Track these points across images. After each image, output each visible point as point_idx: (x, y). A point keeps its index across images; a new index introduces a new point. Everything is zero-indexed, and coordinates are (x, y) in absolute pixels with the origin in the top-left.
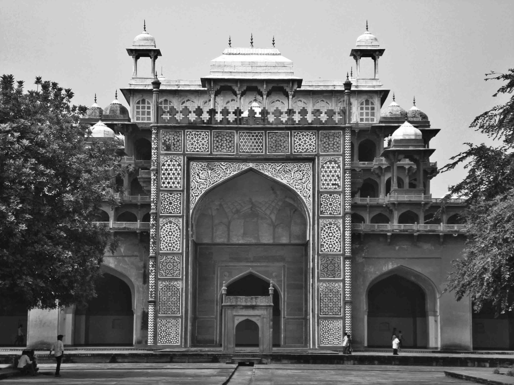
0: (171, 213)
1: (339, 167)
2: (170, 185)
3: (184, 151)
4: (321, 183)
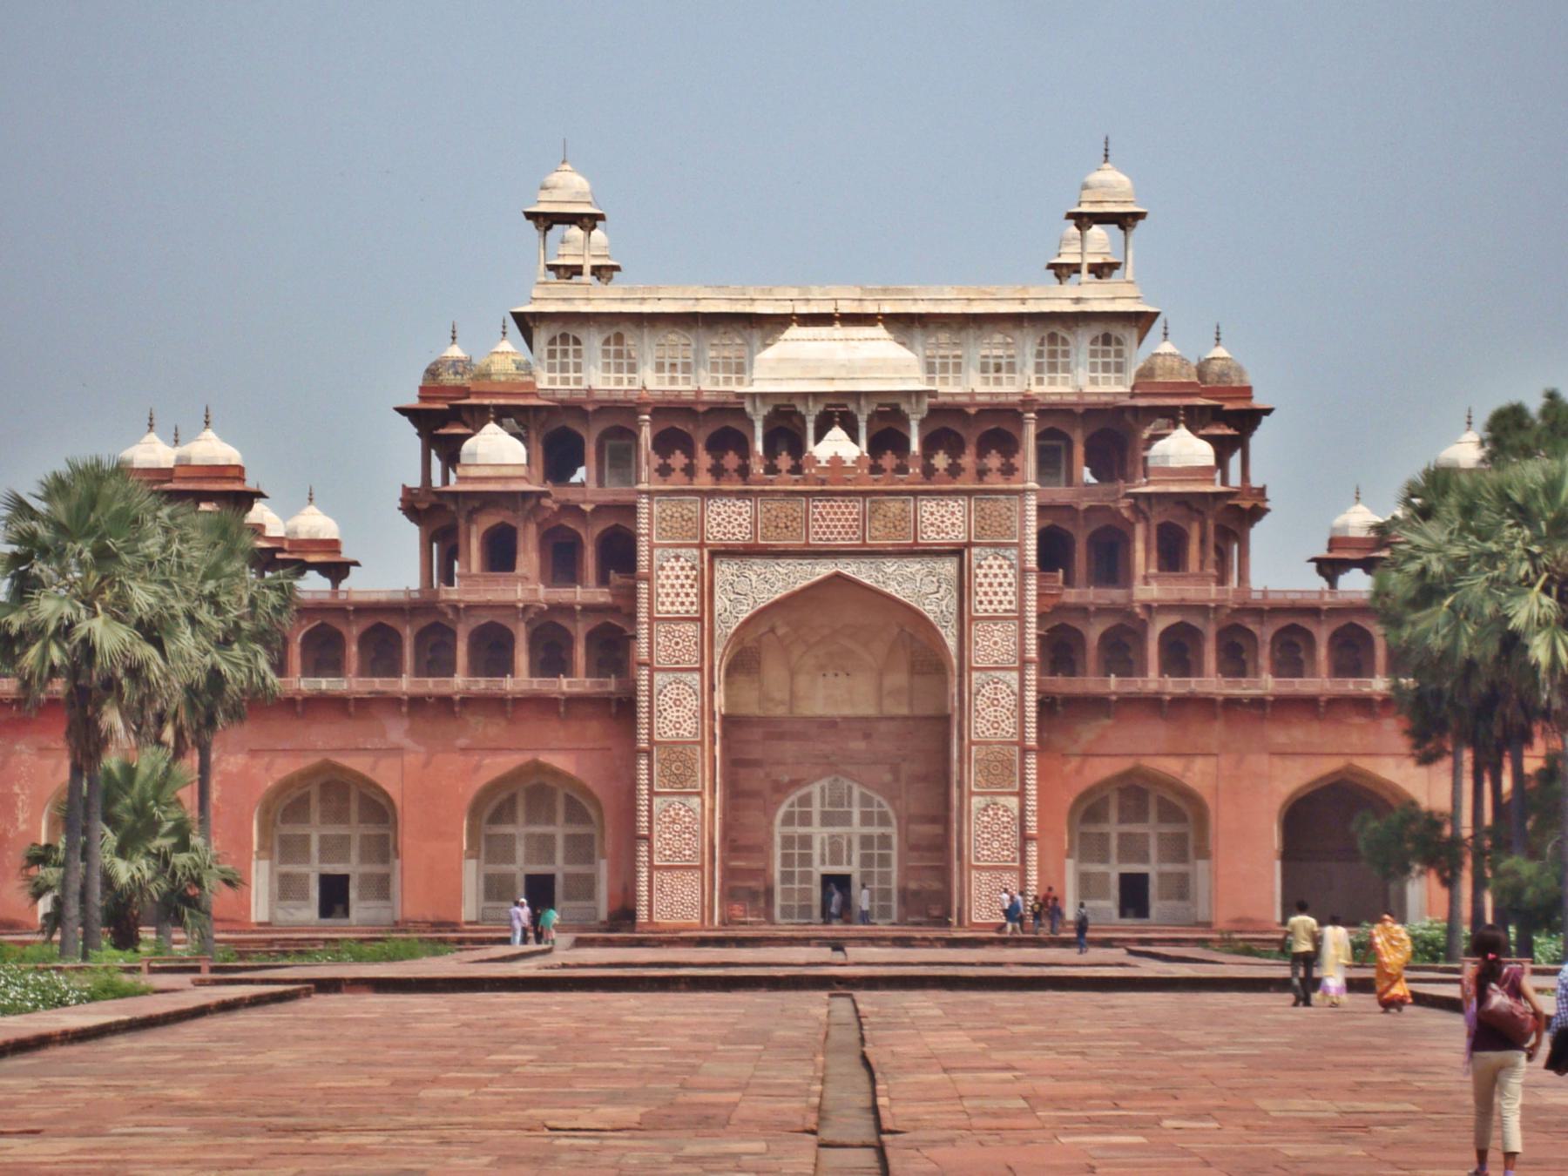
1: (1011, 566)
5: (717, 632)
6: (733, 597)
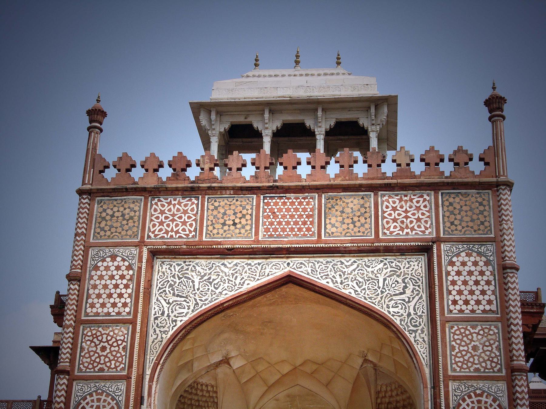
0: (102, 370)
2: (105, 310)
3: (143, 237)
4: (448, 300)
5: (151, 339)
6: (172, 299)
